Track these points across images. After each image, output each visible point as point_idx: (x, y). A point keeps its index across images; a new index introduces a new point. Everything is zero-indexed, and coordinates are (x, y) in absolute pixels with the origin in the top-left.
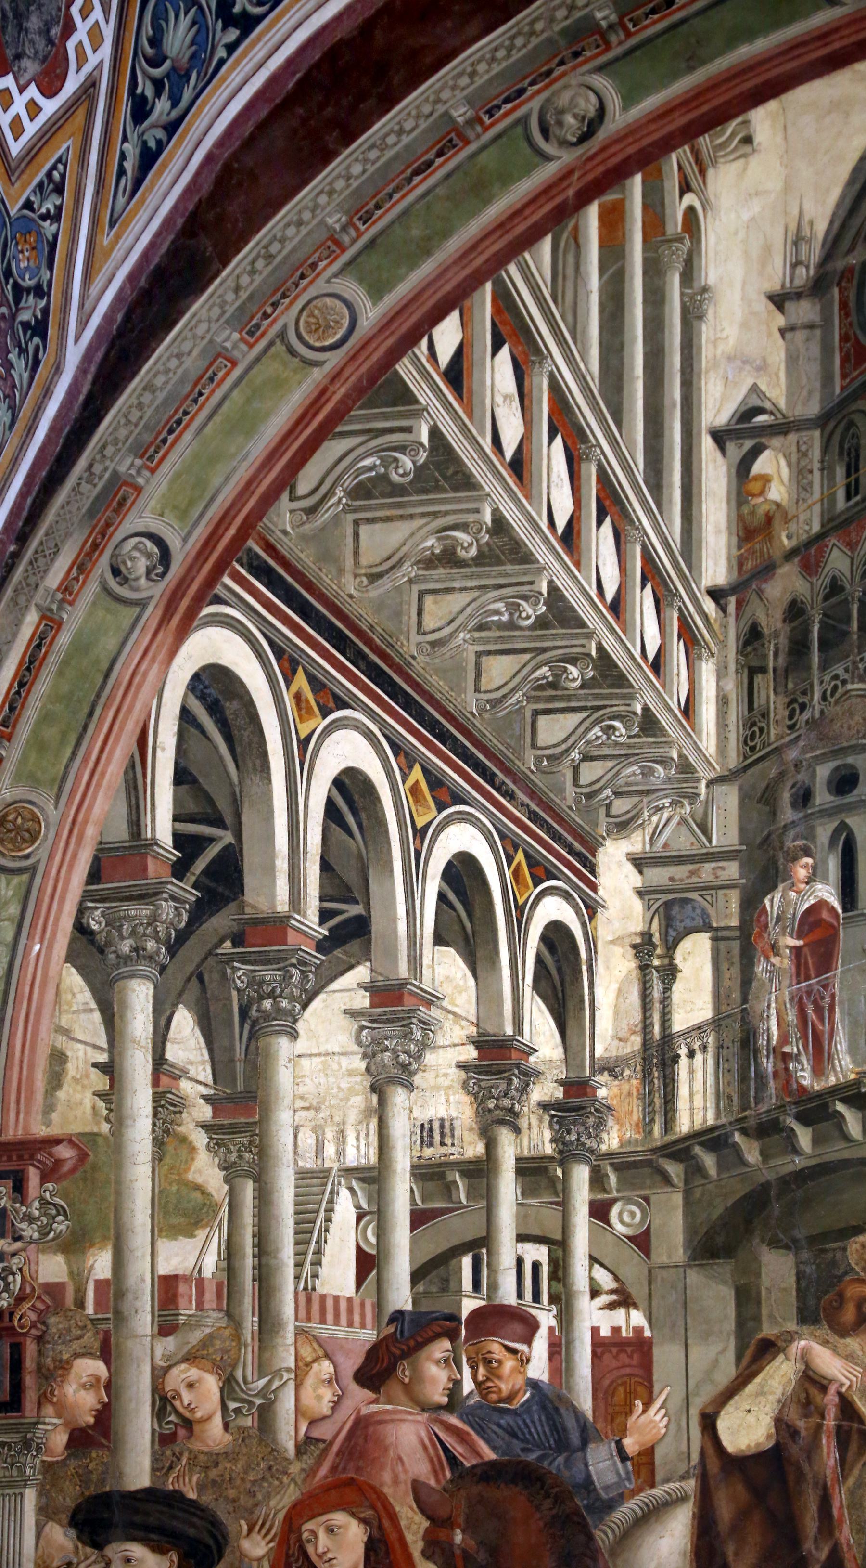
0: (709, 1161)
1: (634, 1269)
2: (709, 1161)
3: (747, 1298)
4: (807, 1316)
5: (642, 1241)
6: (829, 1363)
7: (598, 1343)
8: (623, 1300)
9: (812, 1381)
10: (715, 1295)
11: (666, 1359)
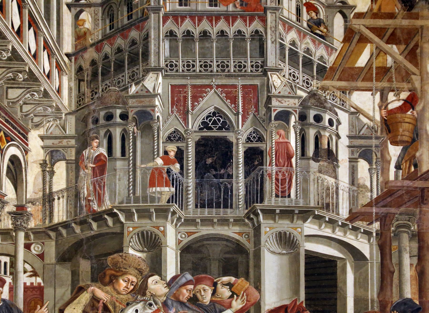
0: (64, 232)
1: (38, 264)
2: (64, 232)
3: (75, 274)
4: (94, 280)
5: (41, 256)
6: (100, 294)
7: (26, 288)
8: (35, 274)
9: (95, 299)
10: (65, 273)
11: (48, 292)
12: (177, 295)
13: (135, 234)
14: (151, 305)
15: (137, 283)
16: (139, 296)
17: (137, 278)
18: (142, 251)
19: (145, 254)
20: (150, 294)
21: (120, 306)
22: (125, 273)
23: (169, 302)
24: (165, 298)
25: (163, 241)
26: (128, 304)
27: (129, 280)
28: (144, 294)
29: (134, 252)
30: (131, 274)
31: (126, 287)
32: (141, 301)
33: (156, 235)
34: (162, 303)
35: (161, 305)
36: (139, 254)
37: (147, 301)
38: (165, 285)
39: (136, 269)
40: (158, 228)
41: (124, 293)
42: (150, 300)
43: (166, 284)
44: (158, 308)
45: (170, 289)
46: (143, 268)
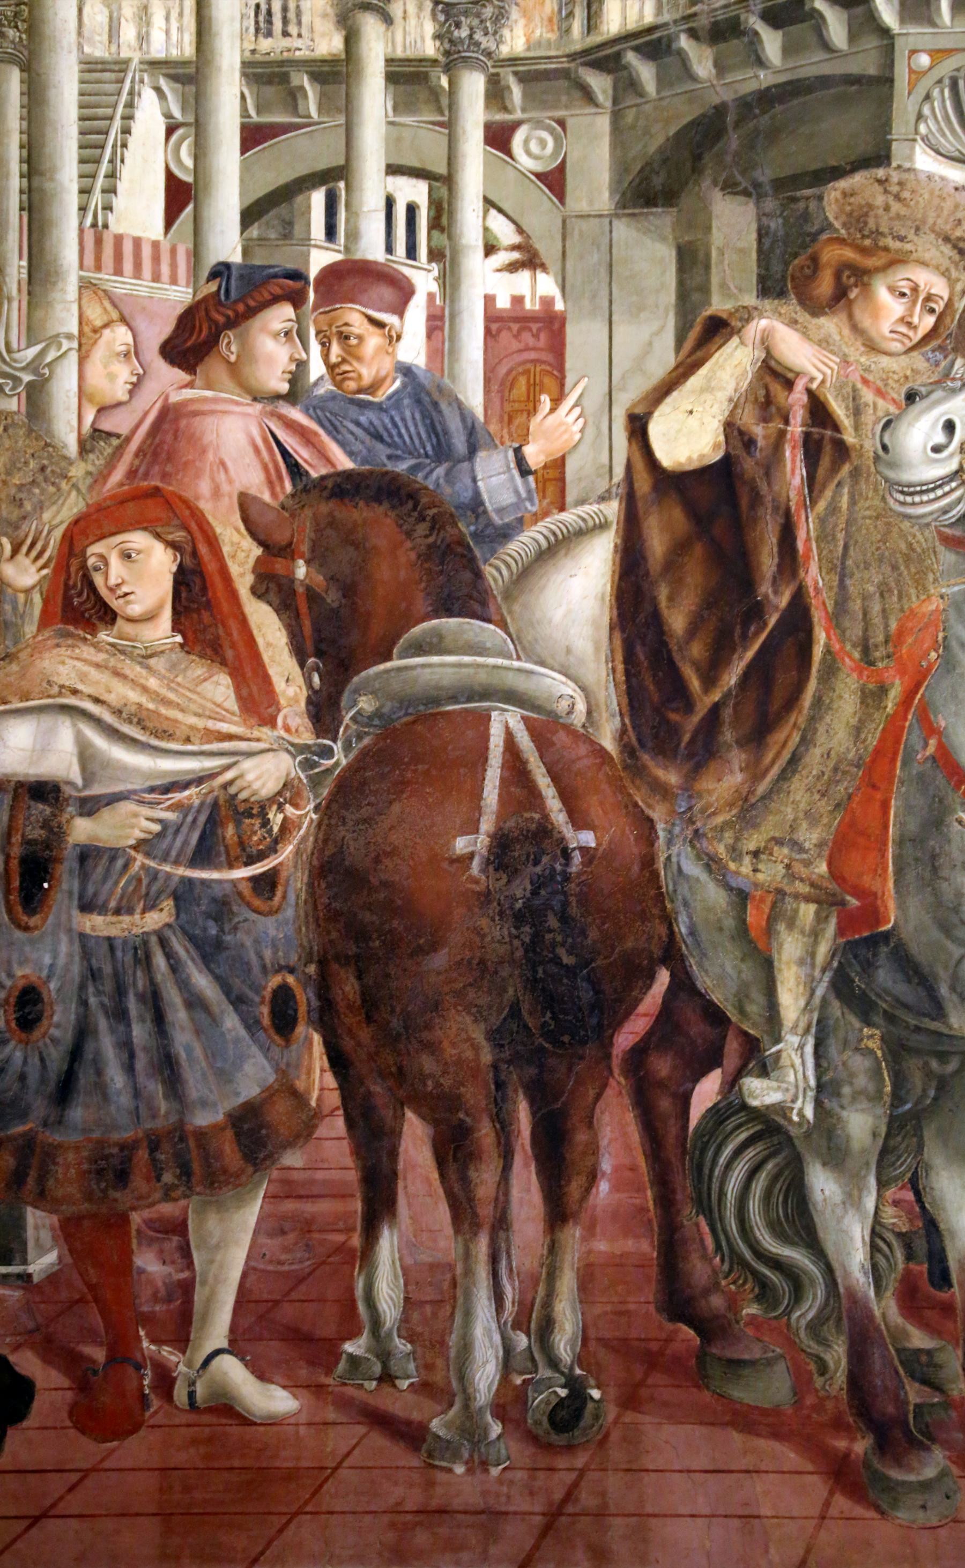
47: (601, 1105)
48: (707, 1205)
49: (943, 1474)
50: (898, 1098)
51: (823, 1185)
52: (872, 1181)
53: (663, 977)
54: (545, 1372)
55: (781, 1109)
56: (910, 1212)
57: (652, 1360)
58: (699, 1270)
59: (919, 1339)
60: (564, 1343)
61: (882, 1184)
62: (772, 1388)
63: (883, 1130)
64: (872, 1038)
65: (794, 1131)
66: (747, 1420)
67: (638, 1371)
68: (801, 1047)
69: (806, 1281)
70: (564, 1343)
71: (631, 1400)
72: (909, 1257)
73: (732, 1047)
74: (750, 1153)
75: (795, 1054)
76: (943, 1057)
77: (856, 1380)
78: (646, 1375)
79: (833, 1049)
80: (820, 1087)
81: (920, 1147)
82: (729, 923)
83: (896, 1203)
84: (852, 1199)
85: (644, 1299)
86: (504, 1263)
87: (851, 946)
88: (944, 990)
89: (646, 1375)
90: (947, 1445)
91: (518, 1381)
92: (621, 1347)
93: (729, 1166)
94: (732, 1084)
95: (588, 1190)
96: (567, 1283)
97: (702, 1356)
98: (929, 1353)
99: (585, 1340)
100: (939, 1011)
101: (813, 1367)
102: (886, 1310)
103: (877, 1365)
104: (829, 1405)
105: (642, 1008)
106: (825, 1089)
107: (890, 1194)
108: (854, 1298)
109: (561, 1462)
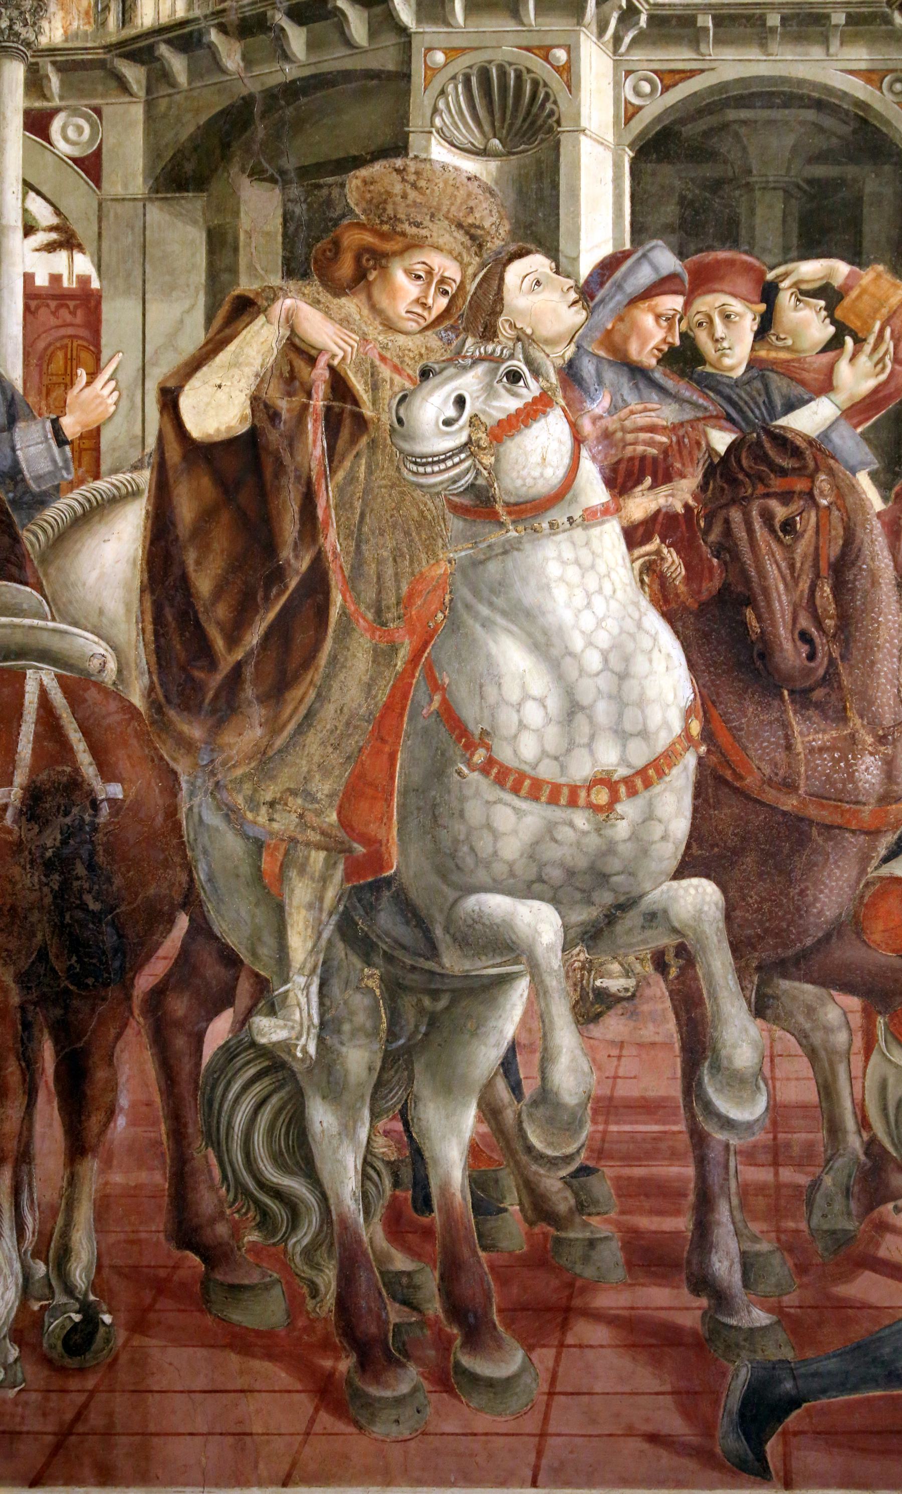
0: (177, 64)
4: (294, 269)
6: (320, 329)
12: (617, 338)
13: (454, 78)
14: (514, 377)
15: (461, 287)
16: (470, 341)
17: (464, 266)
18: (483, 153)
19: (493, 165)
20: (511, 333)
21: (397, 378)
22: (414, 245)
23: (588, 368)
24: (572, 348)
25: (563, 106)
26: (425, 374)
27: (430, 272)
28: (489, 333)
29: (452, 156)
30: (438, 248)
31: (417, 301)
32: (476, 361)
33: (535, 84)
34: (559, 371)
35: (554, 379)
36: (470, 165)
37: (500, 360)
38: (573, 296)
39: (460, 226)
40: (545, 52)
41: (412, 326)
42: (512, 356)
43: (577, 288)
44: (544, 393)
45: (591, 312)
46: (487, 225)
47: (120, 1045)
48: (215, 1139)
49: (415, 1390)
50: (392, 1035)
51: (322, 1117)
52: (366, 1113)
53: (183, 922)
54: (61, 1299)
55: (287, 1046)
56: (399, 1142)
57: (161, 1287)
58: (207, 1200)
59: (401, 1262)
60: (80, 1272)
61: (375, 1116)
62: (268, 1312)
63: (378, 1065)
64: (372, 977)
65: (296, 1067)
66: (243, 1342)
67: (148, 1296)
68: (307, 987)
69: (303, 1209)
70: (80, 1272)
71: (140, 1324)
72: (396, 1184)
73: (244, 987)
74: (257, 1088)
75: (301, 994)
76: (435, 994)
77: (344, 1304)
78: (155, 1300)
79: (336, 989)
80: (323, 1025)
81: (411, 1079)
82: (245, 870)
83: (386, 1133)
84: (348, 1130)
85: (156, 1228)
86: (25, 1195)
87: (357, 891)
88: (438, 931)
89: (155, 1300)
90: (420, 1362)
91: (36, 1307)
92: (133, 1274)
93: (237, 1100)
94: (243, 1022)
95: (106, 1125)
96: (84, 1214)
97: (206, 1281)
98: (409, 1274)
99: (99, 1268)
100: (433, 951)
101: (305, 1290)
102: (373, 1234)
103: (363, 1288)
104: (319, 1326)
105: (161, 952)
106: (328, 1026)
107: (381, 1125)
108: (345, 1224)
109: (74, 1384)
